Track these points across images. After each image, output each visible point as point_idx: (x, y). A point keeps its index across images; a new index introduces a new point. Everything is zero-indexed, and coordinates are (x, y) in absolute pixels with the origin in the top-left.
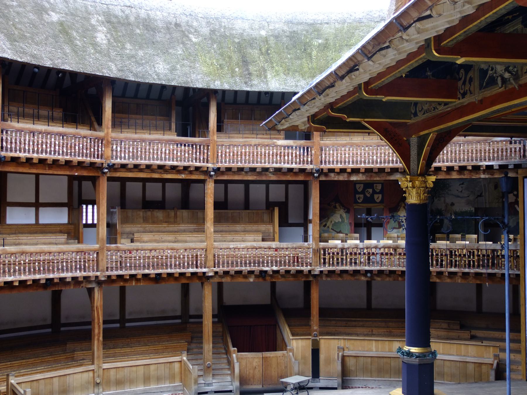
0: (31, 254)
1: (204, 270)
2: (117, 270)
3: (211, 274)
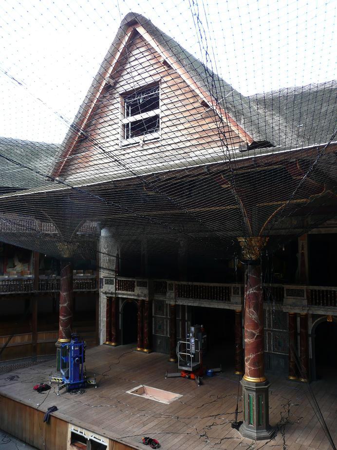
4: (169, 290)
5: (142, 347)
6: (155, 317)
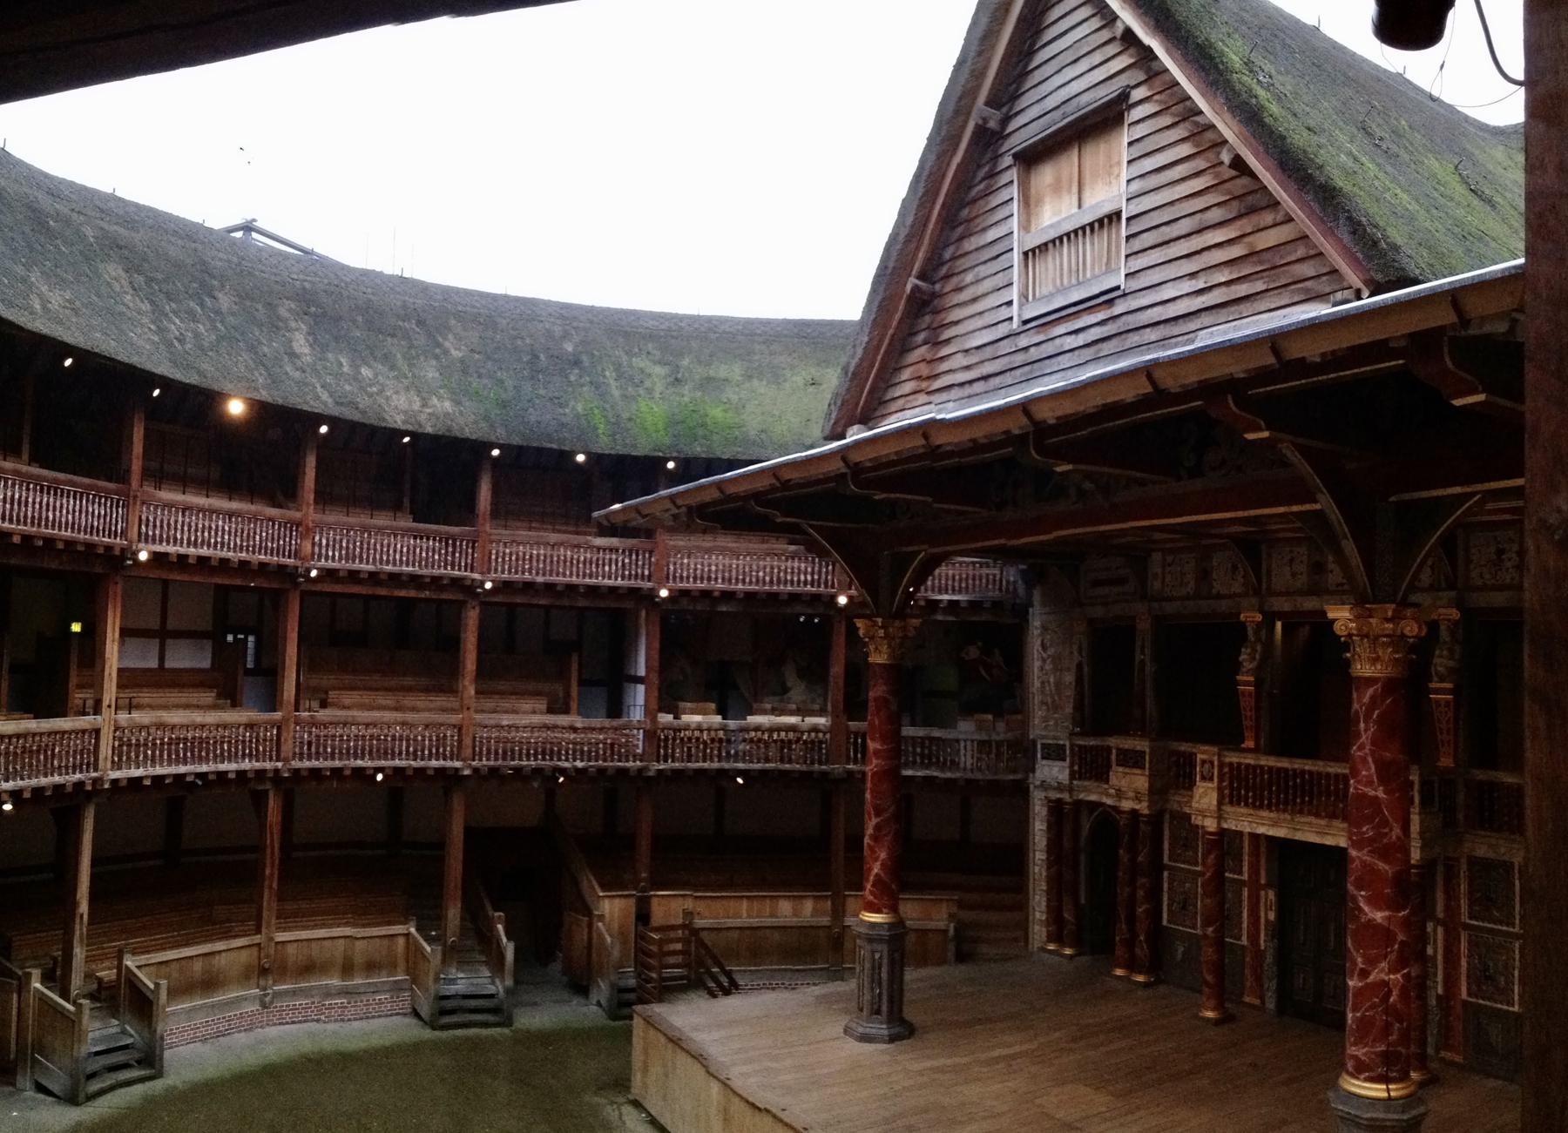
0: (173, 727)
1: (458, 764)
2: (309, 759)
3: (467, 772)
4: (1203, 778)
5: (1132, 966)
6: (1170, 868)
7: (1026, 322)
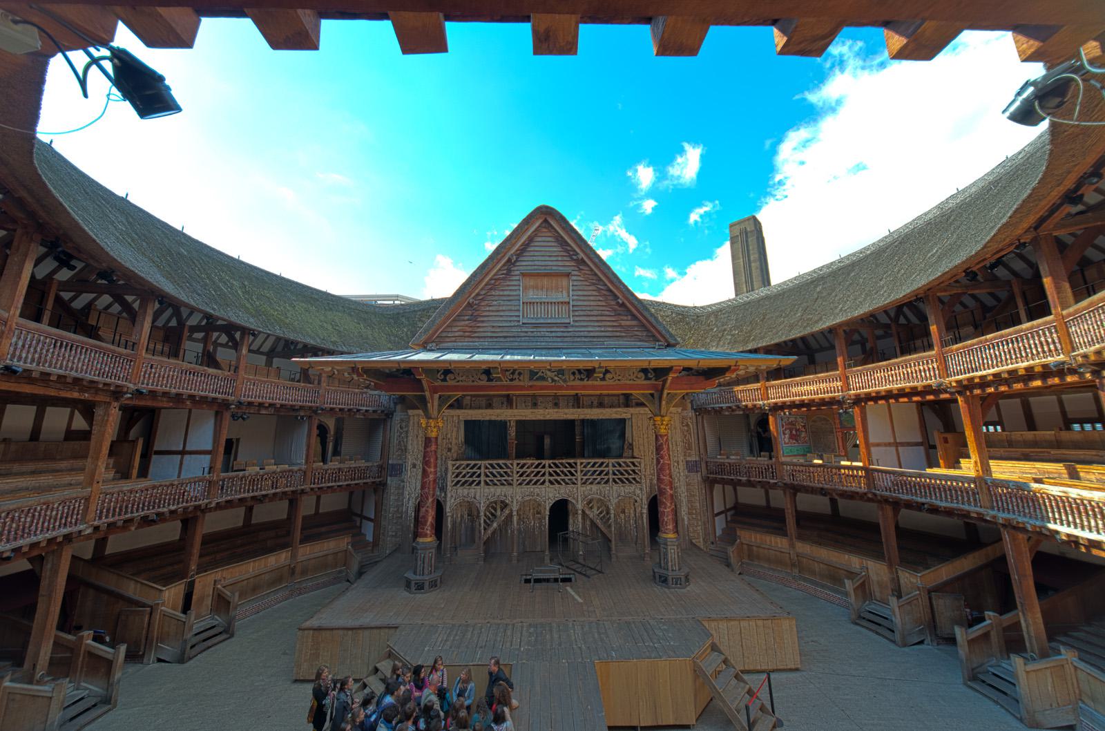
7: (523, 324)
